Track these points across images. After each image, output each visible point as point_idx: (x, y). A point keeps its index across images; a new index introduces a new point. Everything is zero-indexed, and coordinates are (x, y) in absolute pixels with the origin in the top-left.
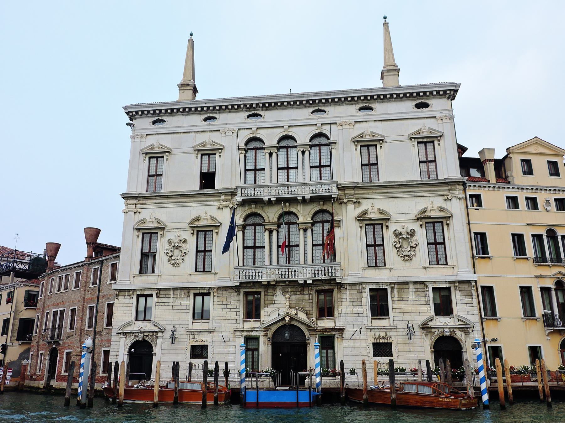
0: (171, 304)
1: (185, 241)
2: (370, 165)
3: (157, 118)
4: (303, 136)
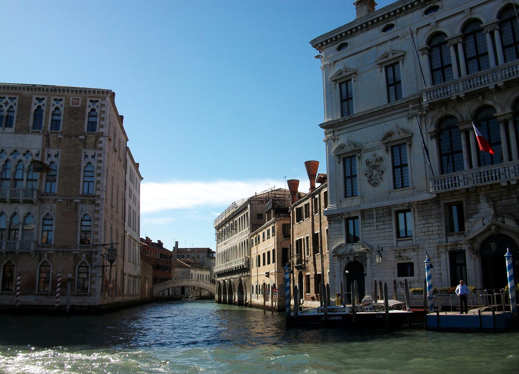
0: (375, 224)
1: (381, 159)
3: (340, 43)
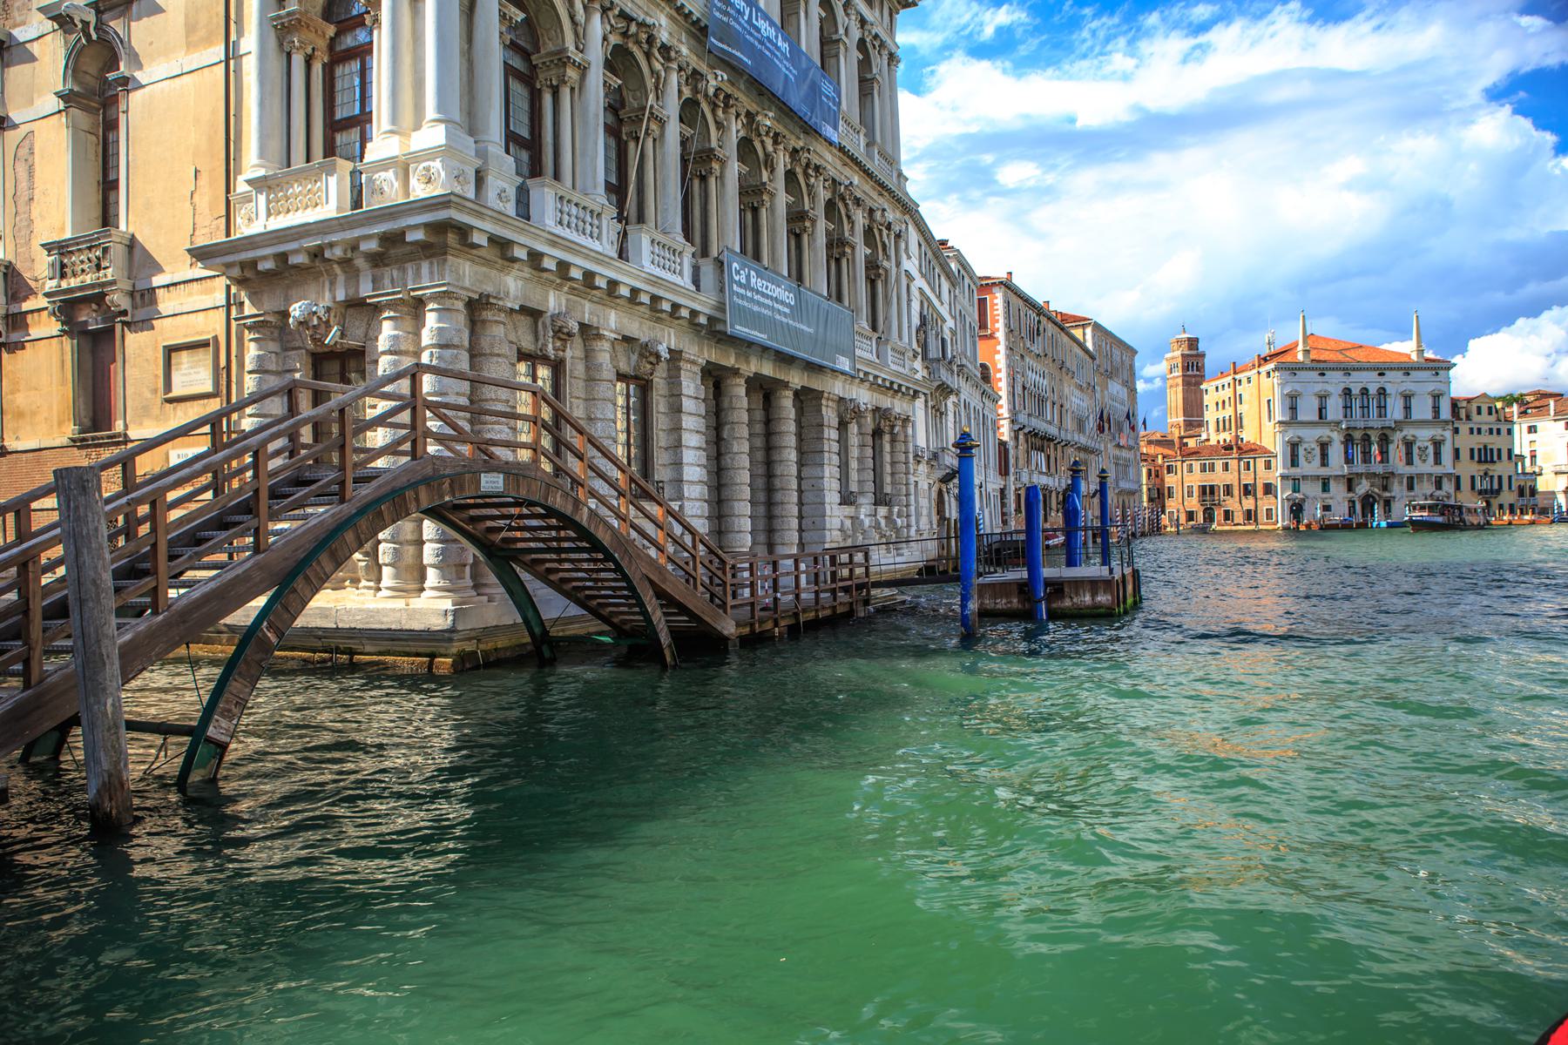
2: (1407, 408)
4: (1373, 390)
